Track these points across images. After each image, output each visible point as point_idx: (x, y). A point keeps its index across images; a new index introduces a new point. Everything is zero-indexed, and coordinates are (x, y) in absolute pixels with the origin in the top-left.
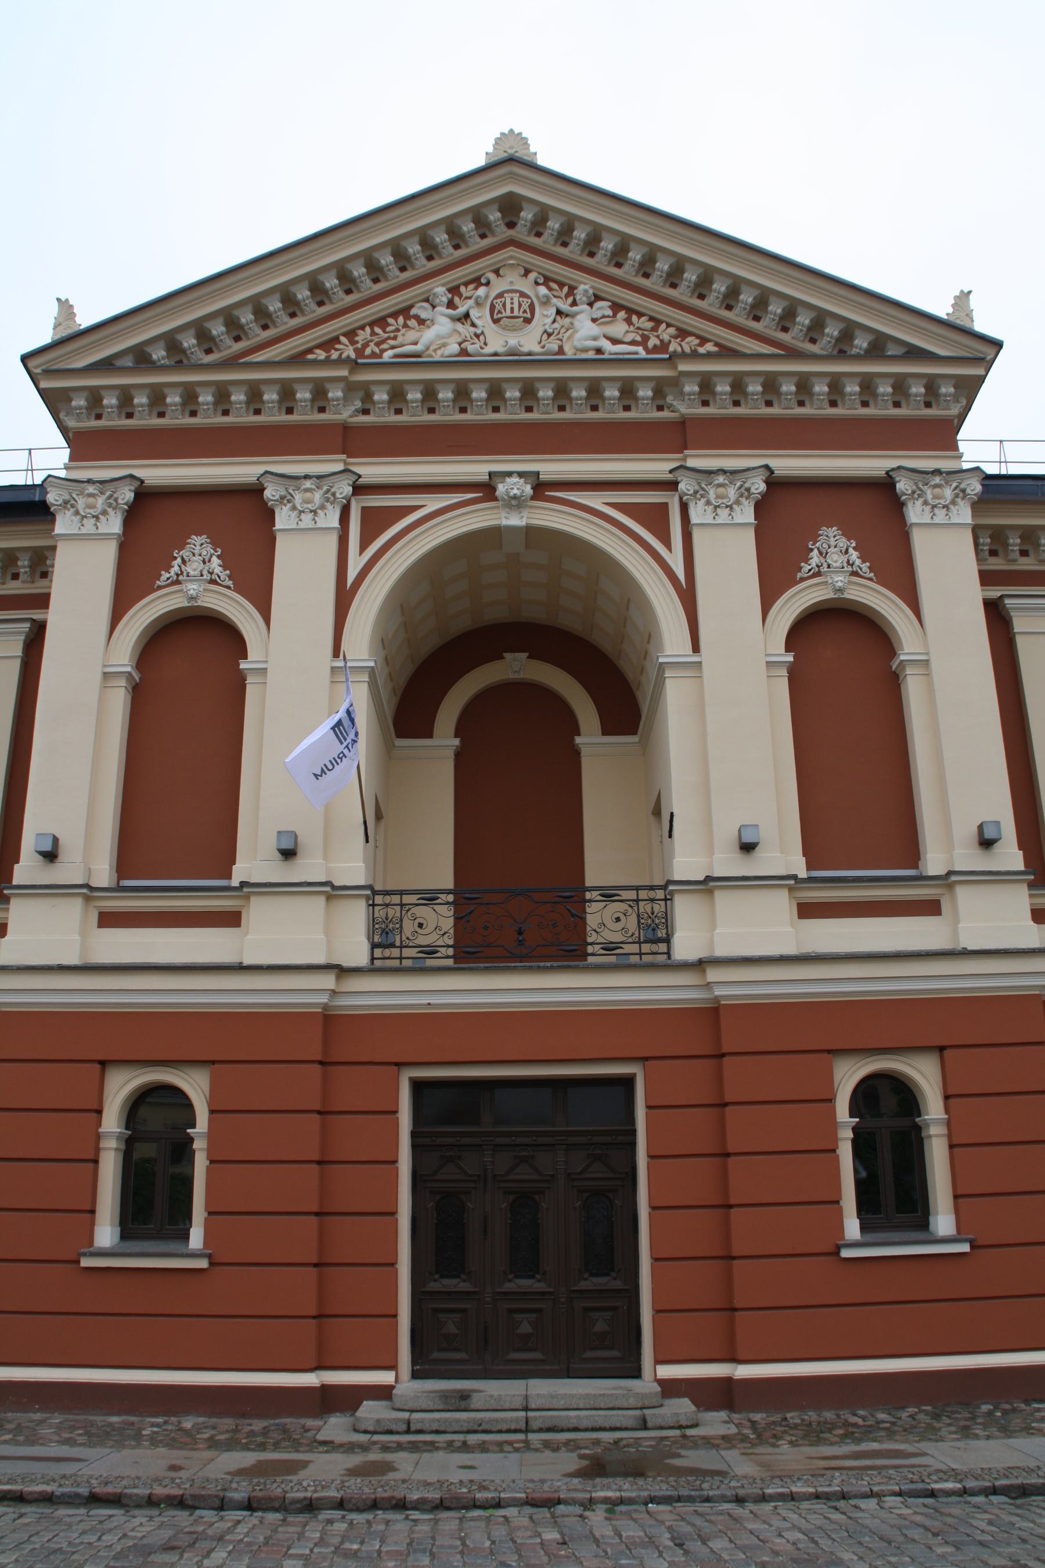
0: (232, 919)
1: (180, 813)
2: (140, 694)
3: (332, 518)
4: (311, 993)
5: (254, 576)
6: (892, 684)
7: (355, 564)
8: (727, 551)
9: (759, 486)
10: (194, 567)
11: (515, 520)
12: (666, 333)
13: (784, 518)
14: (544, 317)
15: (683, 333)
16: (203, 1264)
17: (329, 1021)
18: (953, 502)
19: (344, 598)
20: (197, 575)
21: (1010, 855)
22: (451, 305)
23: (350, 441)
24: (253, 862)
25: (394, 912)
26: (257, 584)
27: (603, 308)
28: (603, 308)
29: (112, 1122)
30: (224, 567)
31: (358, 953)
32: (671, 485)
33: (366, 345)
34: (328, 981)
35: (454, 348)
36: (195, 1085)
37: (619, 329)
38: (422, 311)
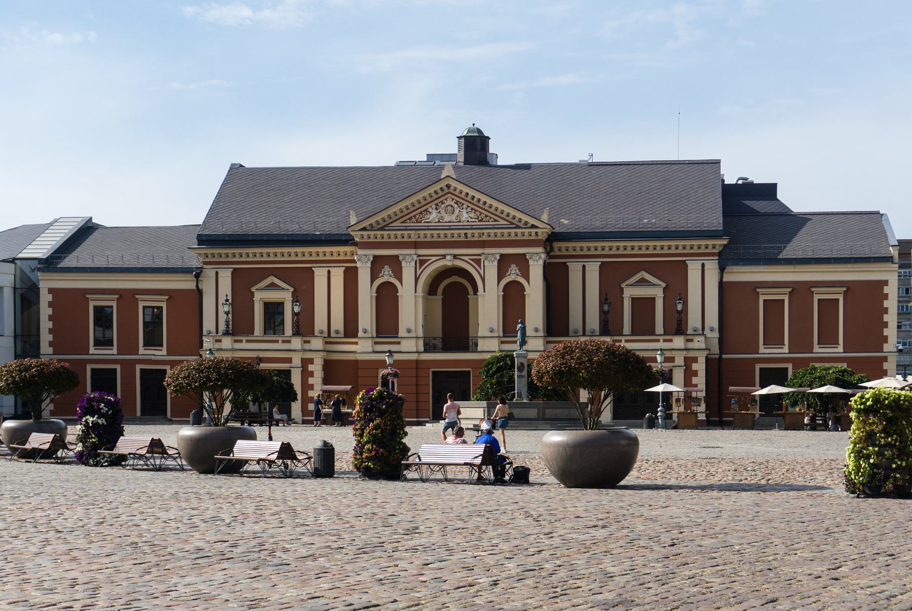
0: (399, 343)
1: (387, 325)
3: (413, 264)
4: (414, 357)
6: (523, 297)
7: (419, 272)
8: (491, 269)
9: (498, 257)
11: (449, 264)
12: (483, 216)
13: (504, 263)
14: (457, 211)
15: (486, 216)
17: (417, 361)
21: (541, 334)
22: (436, 209)
23: (416, 245)
26: (400, 278)
27: (469, 209)
28: (469, 209)
31: (422, 349)
32: (480, 255)
34: (417, 355)
37: (472, 215)
38: (430, 210)
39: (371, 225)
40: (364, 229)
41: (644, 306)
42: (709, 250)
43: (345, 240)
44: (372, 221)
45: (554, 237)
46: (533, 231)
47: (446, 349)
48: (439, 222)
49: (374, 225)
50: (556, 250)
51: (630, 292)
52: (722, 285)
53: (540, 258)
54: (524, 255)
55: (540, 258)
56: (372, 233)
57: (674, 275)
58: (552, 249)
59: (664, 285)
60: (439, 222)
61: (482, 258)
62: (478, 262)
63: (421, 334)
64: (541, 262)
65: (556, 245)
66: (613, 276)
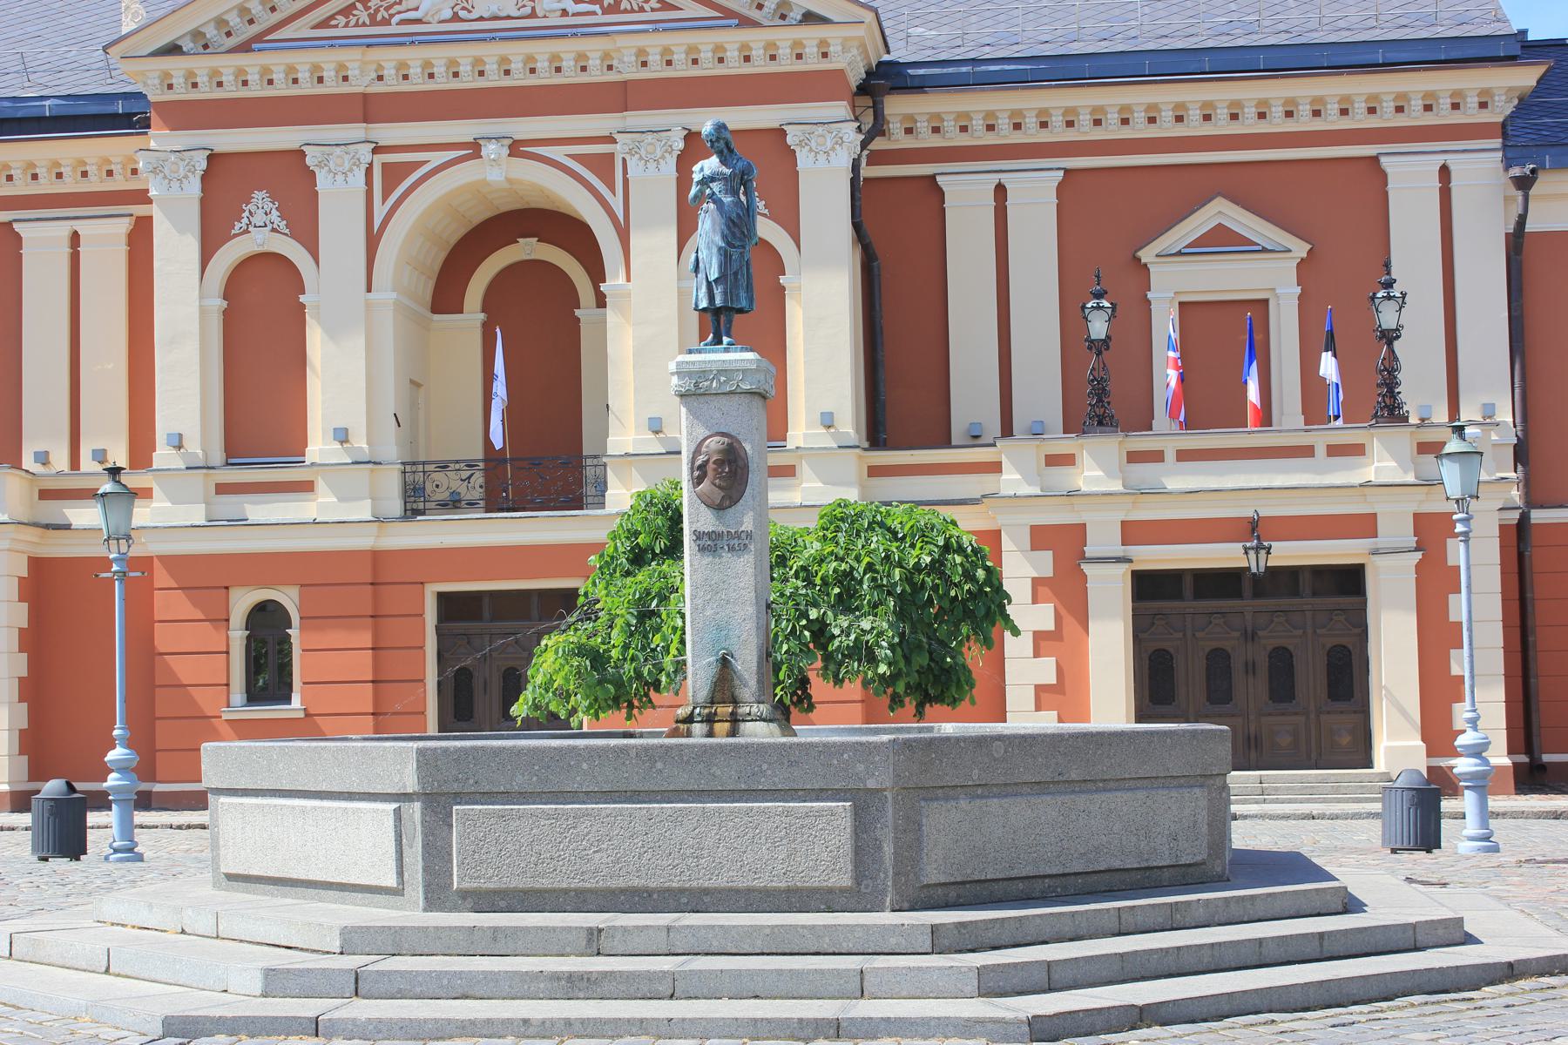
2: (230, 319)
5: (304, 223)
7: (380, 212)
10: (259, 218)
16: (301, 715)
18: (833, 149)
19: (372, 242)
20: (261, 230)
23: (369, 108)
24: (319, 447)
25: (420, 477)
26: (306, 231)
29: (238, 636)
30: (282, 217)
31: (395, 506)
33: (377, 11)
35: (448, 14)
36: (288, 598)
39: (197, 34)
40: (173, 49)
41: (1227, 337)
42: (1471, 115)
43: (119, 116)
44: (199, 17)
45: (883, 81)
46: (812, 33)
47: (496, 501)
48: (456, 18)
49: (211, 32)
50: (896, 127)
51: (1176, 279)
52: (1517, 242)
53: (840, 142)
54: (780, 133)
55: (840, 142)
56: (201, 65)
57: (1335, 209)
58: (878, 128)
59: (1300, 249)
60: (456, 18)
61: (618, 149)
62: (603, 166)
63: (391, 450)
64: (843, 160)
65: (897, 106)
66: (1110, 218)
